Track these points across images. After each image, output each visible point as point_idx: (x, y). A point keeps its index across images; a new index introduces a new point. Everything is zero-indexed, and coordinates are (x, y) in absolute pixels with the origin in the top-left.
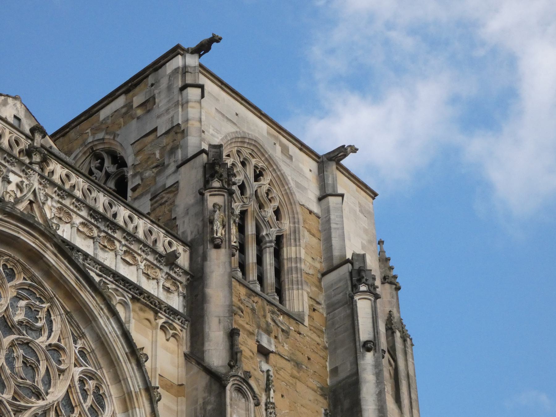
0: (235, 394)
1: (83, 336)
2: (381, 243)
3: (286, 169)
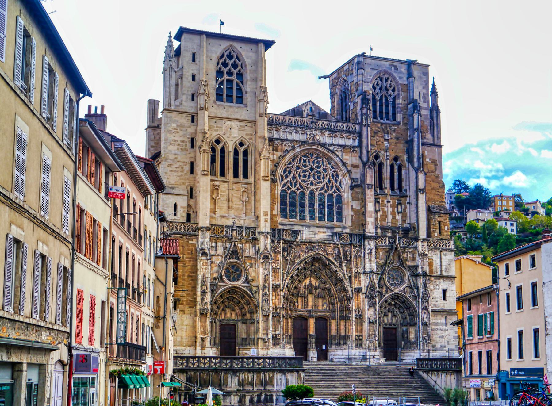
0: (368, 169)
1: (332, 162)
2: (434, 78)
3: (395, 75)
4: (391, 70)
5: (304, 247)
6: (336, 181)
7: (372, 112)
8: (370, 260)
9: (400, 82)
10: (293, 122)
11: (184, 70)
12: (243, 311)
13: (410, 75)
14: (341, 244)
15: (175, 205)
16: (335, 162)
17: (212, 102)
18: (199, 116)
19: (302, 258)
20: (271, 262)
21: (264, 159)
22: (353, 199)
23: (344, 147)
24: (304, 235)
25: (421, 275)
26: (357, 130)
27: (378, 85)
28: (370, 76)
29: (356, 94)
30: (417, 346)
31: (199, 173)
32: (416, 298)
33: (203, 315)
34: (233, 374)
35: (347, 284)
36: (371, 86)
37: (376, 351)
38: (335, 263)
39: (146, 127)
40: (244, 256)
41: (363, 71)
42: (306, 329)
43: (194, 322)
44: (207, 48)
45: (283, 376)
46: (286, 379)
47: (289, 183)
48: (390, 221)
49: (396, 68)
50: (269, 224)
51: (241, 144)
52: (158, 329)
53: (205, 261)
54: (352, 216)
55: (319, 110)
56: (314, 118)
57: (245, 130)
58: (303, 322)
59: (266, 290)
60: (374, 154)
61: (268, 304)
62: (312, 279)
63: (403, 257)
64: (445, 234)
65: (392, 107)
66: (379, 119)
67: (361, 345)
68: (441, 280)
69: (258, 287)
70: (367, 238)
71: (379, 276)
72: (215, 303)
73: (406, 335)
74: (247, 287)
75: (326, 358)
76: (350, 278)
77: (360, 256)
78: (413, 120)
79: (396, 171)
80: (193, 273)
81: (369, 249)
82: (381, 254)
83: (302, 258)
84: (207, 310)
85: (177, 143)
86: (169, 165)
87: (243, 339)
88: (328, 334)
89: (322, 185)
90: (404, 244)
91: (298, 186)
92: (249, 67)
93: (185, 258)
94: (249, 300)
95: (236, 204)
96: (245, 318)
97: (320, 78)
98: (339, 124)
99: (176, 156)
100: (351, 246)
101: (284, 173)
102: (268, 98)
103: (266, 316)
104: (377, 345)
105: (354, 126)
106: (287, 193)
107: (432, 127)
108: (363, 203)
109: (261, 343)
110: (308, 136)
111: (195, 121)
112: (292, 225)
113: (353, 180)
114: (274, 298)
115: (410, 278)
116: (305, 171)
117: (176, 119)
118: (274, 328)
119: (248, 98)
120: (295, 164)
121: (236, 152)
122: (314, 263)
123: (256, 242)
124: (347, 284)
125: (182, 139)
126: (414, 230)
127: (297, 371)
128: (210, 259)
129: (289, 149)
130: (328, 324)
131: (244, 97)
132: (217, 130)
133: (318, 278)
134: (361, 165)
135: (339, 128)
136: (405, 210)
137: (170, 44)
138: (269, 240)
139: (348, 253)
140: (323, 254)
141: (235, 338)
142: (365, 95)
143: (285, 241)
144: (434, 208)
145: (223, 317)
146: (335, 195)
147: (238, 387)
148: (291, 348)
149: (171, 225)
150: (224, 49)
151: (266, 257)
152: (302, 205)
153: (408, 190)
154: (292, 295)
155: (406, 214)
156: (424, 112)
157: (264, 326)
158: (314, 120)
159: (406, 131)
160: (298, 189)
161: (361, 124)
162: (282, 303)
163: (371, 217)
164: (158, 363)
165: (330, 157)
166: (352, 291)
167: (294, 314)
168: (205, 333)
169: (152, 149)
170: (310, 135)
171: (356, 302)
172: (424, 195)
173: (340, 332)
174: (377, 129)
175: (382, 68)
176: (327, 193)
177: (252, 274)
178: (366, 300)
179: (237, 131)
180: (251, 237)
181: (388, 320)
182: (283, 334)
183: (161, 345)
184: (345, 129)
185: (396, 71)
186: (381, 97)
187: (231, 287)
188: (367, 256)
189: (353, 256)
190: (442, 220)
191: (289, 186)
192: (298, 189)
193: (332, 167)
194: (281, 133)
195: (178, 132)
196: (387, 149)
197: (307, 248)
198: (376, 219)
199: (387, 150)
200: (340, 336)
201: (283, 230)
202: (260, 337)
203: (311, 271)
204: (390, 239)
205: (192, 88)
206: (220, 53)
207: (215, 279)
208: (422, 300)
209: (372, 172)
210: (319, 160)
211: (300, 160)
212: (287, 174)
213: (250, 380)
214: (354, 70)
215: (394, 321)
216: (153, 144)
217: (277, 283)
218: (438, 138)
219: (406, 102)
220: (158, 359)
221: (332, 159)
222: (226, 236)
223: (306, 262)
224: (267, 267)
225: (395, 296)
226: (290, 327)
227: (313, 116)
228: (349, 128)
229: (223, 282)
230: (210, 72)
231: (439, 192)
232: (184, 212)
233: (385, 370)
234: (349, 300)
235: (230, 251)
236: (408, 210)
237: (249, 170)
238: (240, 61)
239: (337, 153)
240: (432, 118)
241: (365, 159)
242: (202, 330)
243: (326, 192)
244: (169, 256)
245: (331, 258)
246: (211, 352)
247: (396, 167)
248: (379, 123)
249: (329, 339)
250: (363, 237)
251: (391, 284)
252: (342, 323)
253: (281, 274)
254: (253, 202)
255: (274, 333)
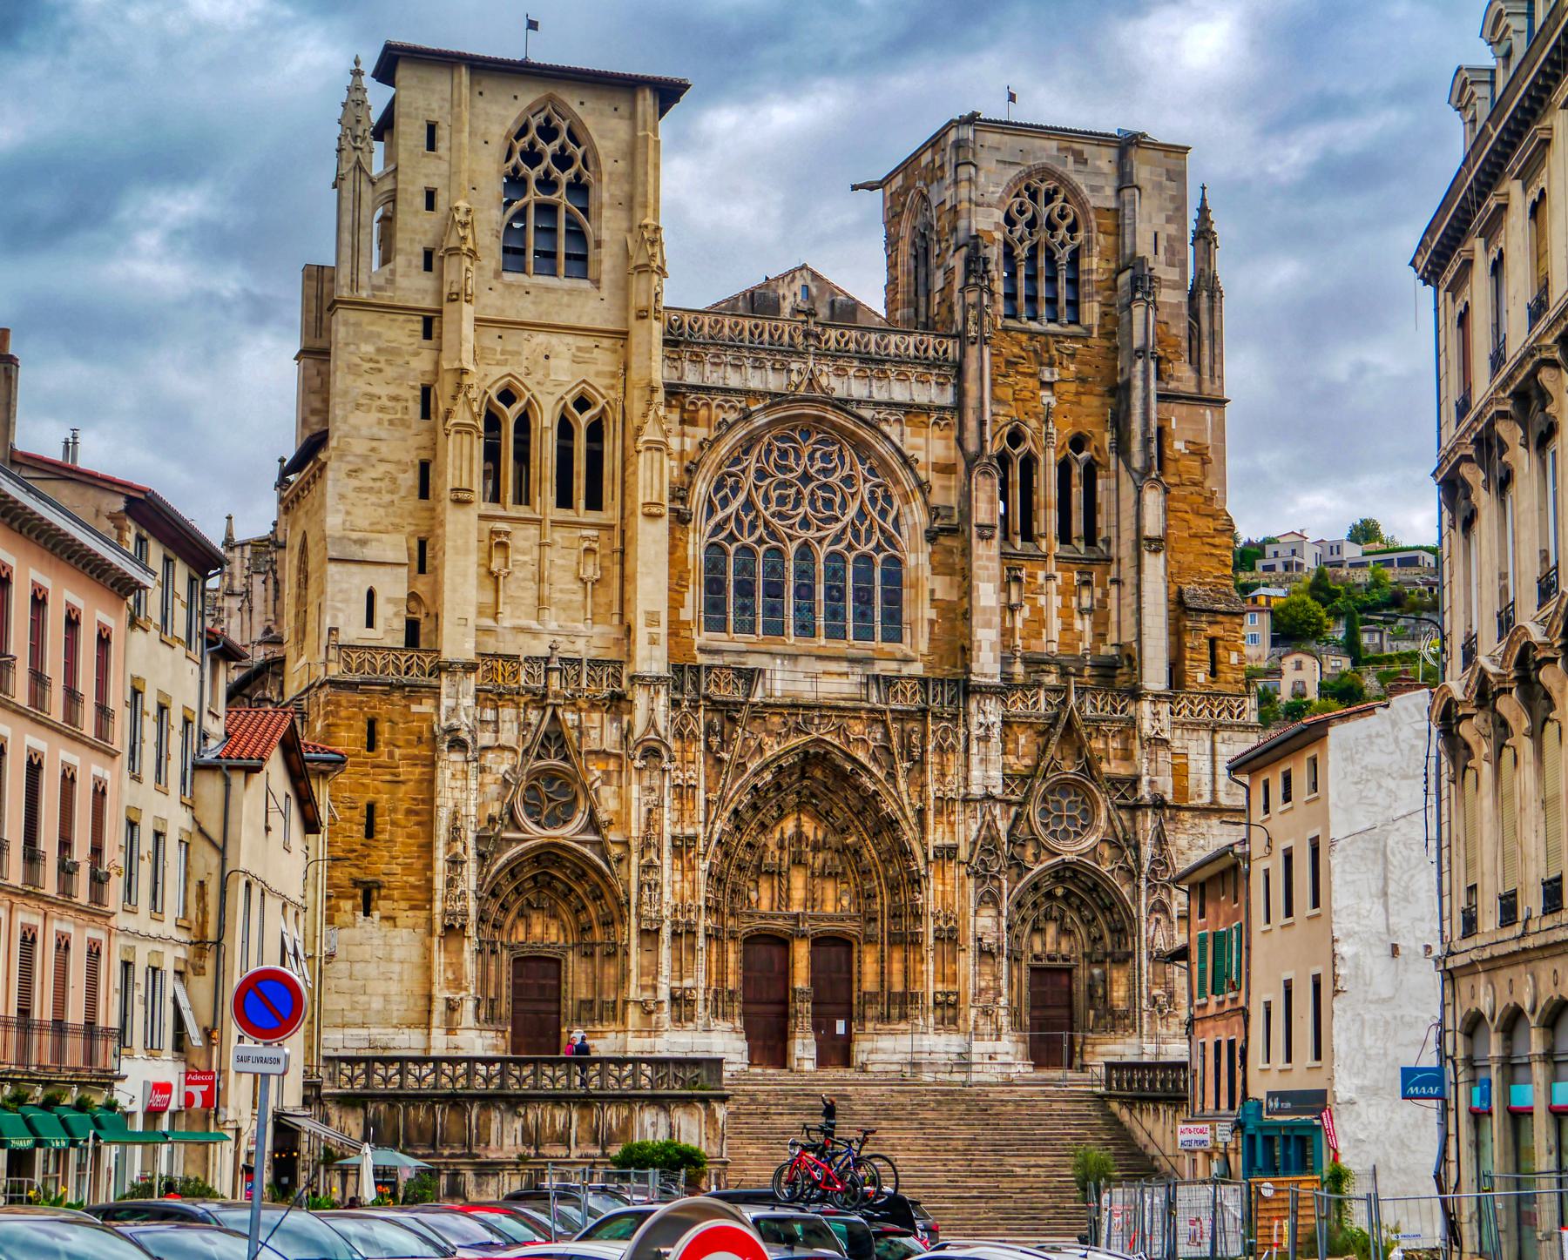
2: (1203, 188)
3: (1078, 180)
4: (1065, 164)
5: (776, 719)
6: (883, 513)
7: (1000, 299)
8: (984, 761)
9: (1094, 201)
10: (747, 333)
11: (400, 177)
12: (583, 917)
13: (1125, 181)
14: (892, 711)
15: (371, 595)
16: (882, 461)
17: (489, 274)
18: (446, 318)
19: (768, 754)
20: (666, 766)
21: (648, 449)
22: (935, 571)
23: (912, 411)
24: (778, 685)
25: (1147, 806)
26: (950, 356)
27: (1021, 212)
28: (997, 185)
29: (952, 242)
30: (1133, 1026)
31: (447, 495)
32: (1131, 875)
33: (453, 931)
34: (508, 1110)
35: (909, 834)
36: (999, 216)
37: (999, 1039)
38: (875, 770)
39: (297, 349)
40: (584, 749)
41: (973, 170)
42: (785, 971)
43: (429, 950)
44: (472, 106)
45: (662, 1115)
46: (671, 1125)
47: (733, 524)
48: (1056, 637)
49: (1080, 159)
50: (661, 652)
51: (582, 404)
52: (201, 978)
53: (459, 766)
54: (932, 622)
55: (833, 293)
56: (812, 321)
57: (594, 362)
58: (776, 951)
59: (652, 854)
60: (1007, 430)
61: (656, 895)
62: (804, 818)
63: (1091, 751)
64: (1230, 677)
65: (1068, 281)
66: (1024, 320)
67: (954, 1020)
68: (1214, 821)
69: (626, 844)
70: (975, 692)
71: (1013, 810)
72: (494, 894)
73: (1100, 991)
74: (592, 843)
75: (847, 1062)
76: (921, 813)
77: (953, 748)
78: (1131, 322)
79: (1075, 480)
80: (423, 801)
81: (981, 725)
82: (1022, 740)
83: (768, 754)
84: (465, 914)
85: (379, 403)
86: (353, 473)
87: (582, 1002)
88: (855, 986)
89: (839, 526)
90: (1095, 708)
91: (761, 531)
92: (607, 165)
93: (397, 756)
94: (598, 886)
95: (561, 591)
96: (588, 938)
97: (855, 188)
98: (894, 338)
99: (374, 444)
100: (925, 717)
101: (716, 493)
102: (663, 261)
103: (650, 935)
104: (1004, 1020)
105: (941, 343)
106: (725, 553)
107: (1195, 343)
108: (966, 584)
109: (633, 1015)
110: (795, 378)
111: (435, 335)
112: (739, 653)
113: (934, 512)
114: (678, 877)
115: (1113, 815)
116: (783, 485)
117: (374, 328)
118: (677, 968)
119: (606, 261)
120: (751, 462)
121: (565, 429)
122: (808, 769)
123: (623, 705)
124: (910, 834)
125: (393, 390)
126: (1130, 665)
127: (705, 1100)
128: (476, 760)
129: (732, 416)
130: (855, 955)
131: (591, 258)
132: (505, 363)
133: (820, 816)
134: (961, 467)
135: (892, 350)
136: (1103, 604)
137: (357, 95)
138: (662, 699)
139: (915, 739)
140: (836, 742)
141: (559, 1001)
142: (976, 248)
143: (714, 703)
144: (1195, 596)
145: (521, 937)
146: (879, 558)
147: (522, 1149)
148: (734, 1030)
149: (354, 656)
150: (530, 108)
151: (652, 753)
152: (774, 590)
153: (1114, 540)
154: (740, 868)
155: (1107, 617)
156: (1167, 296)
157: (645, 963)
158: (811, 326)
159: (1111, 356)
160: (761, 541)
161: (961, 337)
162: (702, 894)
163: (988, 625)
164: (198, 1078)
165: (863, 440)
166: (926, 855)
167: (744, 927)
168: (457, 983)
169: (314, 419)
170: (800, 372)
171: (940, 888)
172: (1162, 555)
173: (890, 982)
174: (1016, 350)
175: (1035, 158)
176: (854, 554)
177: (608, 804)
178: (971, 883)
179: (566, 363)
180: (606, 692)
181: (1044, 944)
182: (708, 989)
183: (208, 1022)
184: (912, 351)
185: (1081, 167)
186: (1034, 249)
187: (542, 846)
188: (974, 749)
189: (930, 748)
190: (1221, 633)
191: (731, 533)
192: (761, 541)
193: (872, 470)
194: (708, 367)
195: (380, 370)
196: (1049, 414)
197: (785, 724)
198: (1007, 633)
199: (1048, 415)
200: (890, 993)
201: (709, 668)
202: (632, 996)
203: (798, 793)
204: (1053, 695)
205: (425, 233)
206: (516, 122)
207: (491, 820)
208: (1148, 880)
209: (993, 486)
210: (830, 449)
211: (769, 452)
212: (726, 496)
213: (559, 1127)
214: (947, 167)
215: (1065, 947)
216: (318, 405)
217: (689, 831)
218: (1212, 376)
219: (1113, 266)
220: (201, 1064)
221: (870, 447)
222: (528, 691)
223: (780, 767)
224: (656, 783)
225: (1065, 869)
226: (731, 965)
227: (811, 313)
228: (926, 350)
229: (519, 828)
230: (481, 182)
231: (1215, 546)
232: (396, 614)
233: (1005, 1097)
234: (918, 882)
235: (540, 736)
236: (1112, 603)
237: (605, 483)
238: (579, 146)
239: (885, 427)
240: (1194, 313)
241: (972, 446)
242: (451, 976)
243: (850, 547)
244: (234, 762)
245: (861, 756)
246: (477, 1041)
247: (1077, 470)
248: (1022, 331)
249: (855, 1001)
250: (966, 689)
251: (1053, 834)
252: (897, 955)
253: (702, 803)
254: (616, 583)
255: (676, 984)
